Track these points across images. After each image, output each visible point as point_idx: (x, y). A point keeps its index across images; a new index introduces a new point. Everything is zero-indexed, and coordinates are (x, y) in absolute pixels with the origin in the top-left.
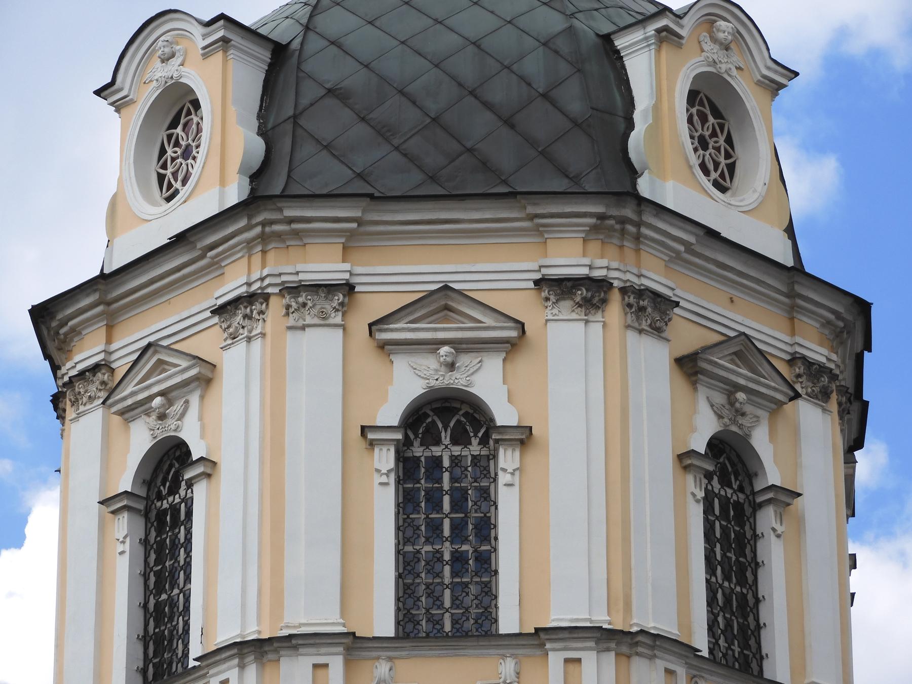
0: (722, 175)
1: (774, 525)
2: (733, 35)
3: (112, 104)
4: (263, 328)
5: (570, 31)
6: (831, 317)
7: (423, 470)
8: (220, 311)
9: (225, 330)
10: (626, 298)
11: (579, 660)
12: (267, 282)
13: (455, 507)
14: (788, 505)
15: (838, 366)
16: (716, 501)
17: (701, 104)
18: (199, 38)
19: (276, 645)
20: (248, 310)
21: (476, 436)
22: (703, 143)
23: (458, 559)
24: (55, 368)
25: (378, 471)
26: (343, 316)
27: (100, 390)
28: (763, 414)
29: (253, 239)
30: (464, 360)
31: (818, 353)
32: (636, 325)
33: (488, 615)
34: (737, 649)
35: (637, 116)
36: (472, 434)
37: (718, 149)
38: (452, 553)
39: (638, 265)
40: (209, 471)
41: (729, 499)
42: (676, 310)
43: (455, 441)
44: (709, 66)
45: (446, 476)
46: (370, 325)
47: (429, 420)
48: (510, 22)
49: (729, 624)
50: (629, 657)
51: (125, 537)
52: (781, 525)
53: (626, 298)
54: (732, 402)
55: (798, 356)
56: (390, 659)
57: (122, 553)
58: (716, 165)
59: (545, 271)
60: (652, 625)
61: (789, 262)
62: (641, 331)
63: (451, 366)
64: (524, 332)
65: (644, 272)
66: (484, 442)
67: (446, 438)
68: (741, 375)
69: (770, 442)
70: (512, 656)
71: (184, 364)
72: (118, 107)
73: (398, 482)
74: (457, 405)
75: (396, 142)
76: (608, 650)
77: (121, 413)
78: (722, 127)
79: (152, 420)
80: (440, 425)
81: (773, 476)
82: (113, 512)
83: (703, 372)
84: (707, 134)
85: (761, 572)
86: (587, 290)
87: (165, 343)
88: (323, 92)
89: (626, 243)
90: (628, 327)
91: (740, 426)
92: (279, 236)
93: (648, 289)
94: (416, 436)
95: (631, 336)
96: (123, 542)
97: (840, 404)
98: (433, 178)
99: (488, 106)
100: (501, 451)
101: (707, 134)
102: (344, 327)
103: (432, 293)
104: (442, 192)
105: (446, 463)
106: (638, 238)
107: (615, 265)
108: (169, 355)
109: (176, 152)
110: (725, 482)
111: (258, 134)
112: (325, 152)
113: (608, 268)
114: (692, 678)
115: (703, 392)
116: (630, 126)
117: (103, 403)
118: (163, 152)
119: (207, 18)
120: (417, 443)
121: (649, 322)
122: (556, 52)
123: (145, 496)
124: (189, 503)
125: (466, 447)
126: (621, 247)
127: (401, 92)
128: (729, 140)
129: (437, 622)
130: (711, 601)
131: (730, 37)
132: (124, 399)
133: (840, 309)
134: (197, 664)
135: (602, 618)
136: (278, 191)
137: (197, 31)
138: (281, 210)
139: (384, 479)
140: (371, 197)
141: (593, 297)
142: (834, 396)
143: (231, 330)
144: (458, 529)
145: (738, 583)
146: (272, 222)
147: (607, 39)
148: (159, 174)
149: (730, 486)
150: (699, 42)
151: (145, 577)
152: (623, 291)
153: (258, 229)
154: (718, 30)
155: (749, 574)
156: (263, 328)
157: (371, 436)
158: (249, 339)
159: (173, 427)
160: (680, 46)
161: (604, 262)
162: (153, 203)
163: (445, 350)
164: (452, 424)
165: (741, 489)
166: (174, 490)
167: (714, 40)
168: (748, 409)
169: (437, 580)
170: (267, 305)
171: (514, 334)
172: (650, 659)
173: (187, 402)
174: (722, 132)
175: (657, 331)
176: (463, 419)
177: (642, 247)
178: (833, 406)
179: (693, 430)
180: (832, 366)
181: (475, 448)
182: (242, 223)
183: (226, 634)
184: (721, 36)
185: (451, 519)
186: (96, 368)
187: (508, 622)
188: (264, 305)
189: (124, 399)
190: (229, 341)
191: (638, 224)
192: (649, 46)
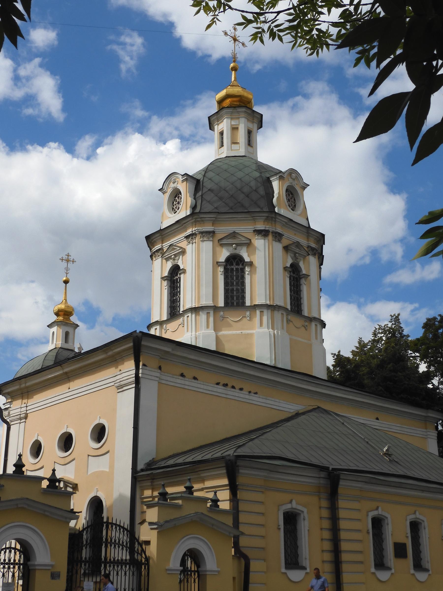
0: (293, 207)
1: (304, 282)
2: (295, 177)
3: (162, 193)
4: (195, 241)
5: (261, 176)
6: (316, 238)
7: (230, 271)
8: (187, 237)
9: (187, 241)
10: (273, 234)
11: (263, 311)
12: (196, 231)
13: (237, 279)
14: (307, 278)
15: (318, 248)
16: (292, 277)
17: (289, 192)
18: (181, 178)
19: (199, 308)
20: (192, 237)
21: (241, 264)
22: (289, 200)
23: (237, 290)
24: (151, 249)
25: (220, 271)
26: (212, 238)
27: (161, 254)
28: (302, 258)
29: (193, 222)
30: (239, 248)
31: (313, 245)
32: (275, 240)
33: (244, 303)
34: (296, 309)
35: (275, 195)
36: (240, 263)
37: (292, 202)
38: (236, 289)
39: (275, 226)
40: (184, 271)
41: (294, 277)
42: (283, 236)
43: (236, 265)
44: (290, 184)
45: (235, 272)
46: (218, 240)
47: (231, 260)
48: (247, 174)
49: (295, 304)
50: (274, 311)
51: (166, 286)
52: (306, 282)
53: (273, 234)
54: (295, 256)
55: (309, 246)
56: (223, 311)
57: (166, 289)
58: (292, 205)
59: (255, 228)
60: (278, 304)
61: (307, 226)
62: (276, 241)
63: (236, 249)
64: (251, 241)
65: (277, 228)
66: (243, 265)
67: (234, 264)
68: (297, 250)
70: (249, 311)
71: (179, 249)
72: (164, 193)
73: (224, 274)
75: (223, 201)
76: (269, 309)
77: (165, 259)
78: (293, 197)
79: (172, 260)
80: (233, 262)
81: (304, 272)
82: (163, 280)
83: (289, 250)
84: (290, 198)
85: (301, 292)
86: (265, 233)
87: (174, 244)
88: (208, 190)
89: (273, 222)
90: (273, 240)
91: (297, 261)
92: (198, 221)
93: (277, 232)
94: (228, 264)
95: (274, 242)
96: (166, 287)
97: (318, 256)
98: (231, 208)
99: (243, 193)
100: (246, 267)
101: (290, 198)
102: (213, 241)
103: (231, 233)
104: (233, 211)
105: (235, 269)
106: (275, 221)
107: (270, 227)
108: (175, 247)
109: (176, 203)
110: (294, 273)
111: (194, 199)
112: (208, 203)
113: (269, 228)
114: (287, 315)
115: (289, 254)
116: (273, 197)
117: (161, 257)
119: (183, 174)
120: (228, 265)
122: (258, 181)
123: (170, 276)
124: (180, 278)
125: (239, 266)
126: (272, 223)
127: (224, 190)
128: (295, 200)
129: (233, 304)
130: (291, 299)
131: (295, 178)
132: (166, 256)
134: (182, 312)
135: (268, 302)
136: (198, 212)
137: (180, 177)
138: (199, 216)
139: (221, 273)
140: (218, 212)
141: (266, 234)
142: (317, 255)
143: (189, 241)
144: (237, 284)
145: (297, 295)
146: (197, 218)
147: (268, 178)
149: (295, 274)
150: (288, 179)
151: (171, 294)
152: (272, 232)
153: (194, 220)
154: (292, 176)
155: (299, 293)
156: (195, 241)
158: (192, 243)
159: (176, 262)
160: (284, 179)
161: (268, 226)
162: (172, 214)
163: (234, 245)
164: (236, 261)
165: (297, 275)
166: (177, 275)
167: (291, 178)
168: (299, 257)
169: (233, 294)
170: (196, 236)
171: (248, 242)
172: (278, 311)
173: (179, 257)
174: (293, 198)
175: (279, 241)
176: (238, 260)
177: (276, 223)
178: (317, 256)
179: (287, 262)
180: (317, 248)
181: (241, 266)
182: (191, 219)
183: (188, 306)
184: (293, 177)
186: (159, 249)
187: (248, 303)
188: (195, 236)
189: (166, 256)
190: (188, 244)
191: (275, 218)
192: (277, 180)
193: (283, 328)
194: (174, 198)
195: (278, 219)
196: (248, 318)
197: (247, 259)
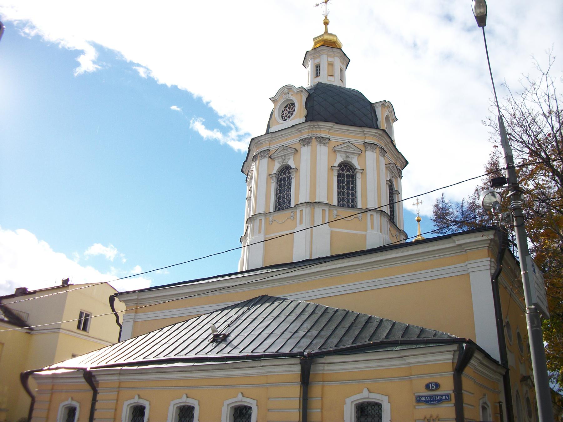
30: (350, 156)
62: (381, 156)
74: (348, 165)
87: (286, 146)
102: (328, 146)
118: (283, 112)
148: (282, 116)
157: (333, 168)
185: (347, 186)
187: (359, 205)
193: (388, 234)
194: (285, 108)
197: (357, 166)
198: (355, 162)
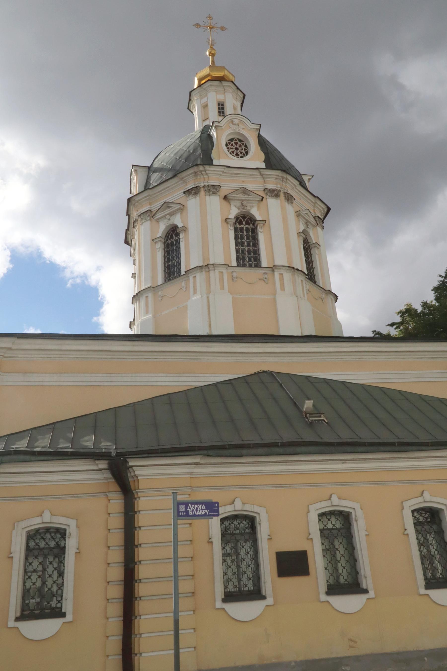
25: (157, 249)
54: (242, 205)
63: (170, 219)
69: (258, 211)
78: (243, 144)
91: (246, 209)
95: (207, 197)
121: (212, 192)
128: (246, 146)
133: (278, 174)
141: (196, 191)
152: (204, 187)
179: (230, 213)
191: (205, 171)
195: (209, 170)
196: (184, 290)
198: (178, 221)
